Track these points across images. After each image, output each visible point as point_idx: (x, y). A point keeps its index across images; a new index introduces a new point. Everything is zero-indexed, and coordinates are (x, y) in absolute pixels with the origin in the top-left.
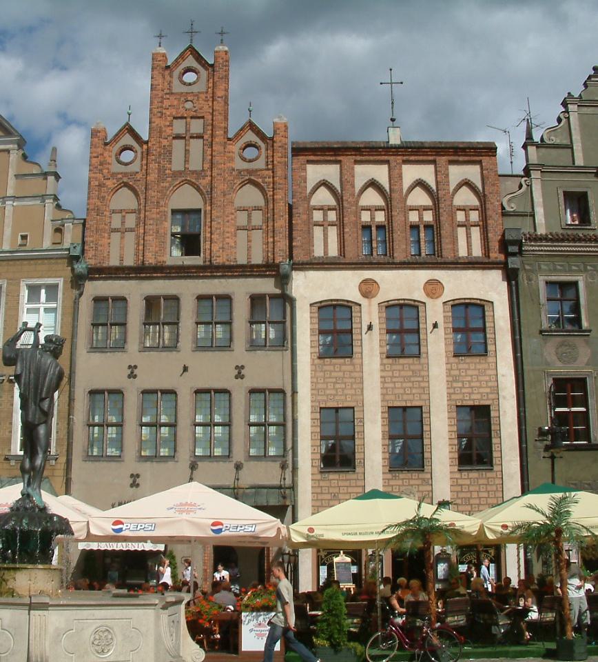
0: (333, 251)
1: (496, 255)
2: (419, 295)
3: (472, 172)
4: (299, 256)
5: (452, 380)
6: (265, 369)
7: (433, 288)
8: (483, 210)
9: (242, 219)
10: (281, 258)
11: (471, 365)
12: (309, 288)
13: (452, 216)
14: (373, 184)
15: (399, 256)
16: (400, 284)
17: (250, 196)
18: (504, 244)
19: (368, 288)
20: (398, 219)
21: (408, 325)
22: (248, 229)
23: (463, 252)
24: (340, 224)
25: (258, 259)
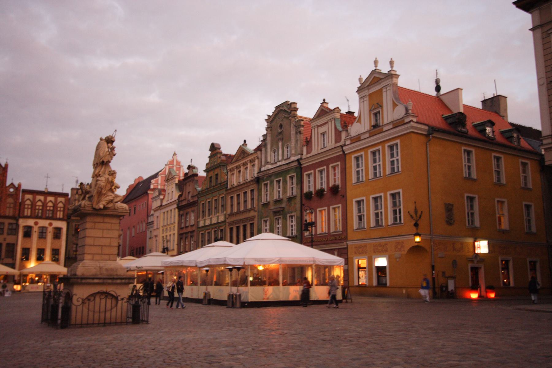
0: (29, 214)
1: (66, 218)
2: (47, 225)
3: (62, 199)
4: (21, 215)
5: (52, 243)
6: (10, 239)
7: (51, 224)
8: (64, 208)
9: (8, 205)
10: (17, 215)
11: (57, 241)
12: (23, 223)
13: (57, 209)
14: (40, 200)
15: (44, 217)
16: (43, 223)
17: (10, 200)
18: (67, 216)
19: (36, 223)
20: (45, 209)
21: (44, 231)
22: (10, 208)
23: (58, 217)
24: (31, 208)
25: (11, 214)
